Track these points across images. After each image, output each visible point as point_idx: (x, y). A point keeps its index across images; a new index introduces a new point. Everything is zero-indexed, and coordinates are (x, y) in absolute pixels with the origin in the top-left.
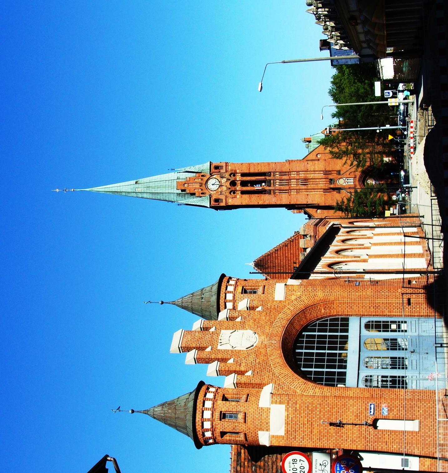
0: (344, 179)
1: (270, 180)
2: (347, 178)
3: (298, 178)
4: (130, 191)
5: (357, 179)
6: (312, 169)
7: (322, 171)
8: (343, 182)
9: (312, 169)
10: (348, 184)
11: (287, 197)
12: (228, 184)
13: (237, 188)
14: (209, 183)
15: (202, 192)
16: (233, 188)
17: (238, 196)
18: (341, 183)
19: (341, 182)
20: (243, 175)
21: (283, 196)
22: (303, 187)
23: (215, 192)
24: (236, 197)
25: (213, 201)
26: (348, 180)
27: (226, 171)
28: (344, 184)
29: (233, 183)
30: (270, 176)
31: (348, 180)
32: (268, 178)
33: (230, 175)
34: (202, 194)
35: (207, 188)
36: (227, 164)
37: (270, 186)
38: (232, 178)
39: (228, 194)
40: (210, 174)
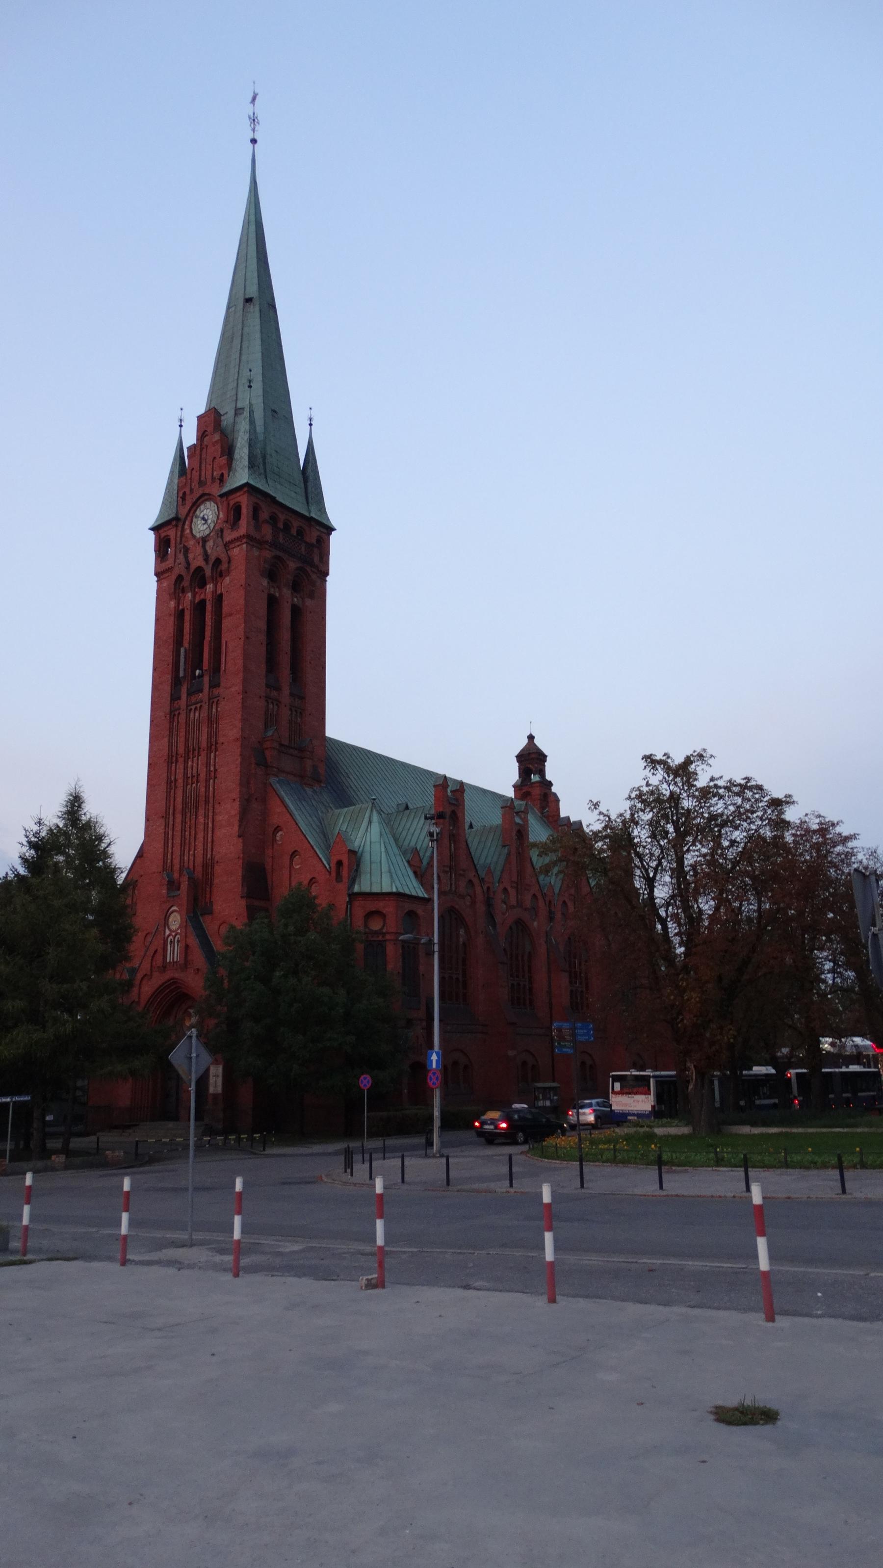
1: (201, 691)
3: (203, 776)
6: (221, 818)
9: (221, 818)
12: (199, 562)
15: (188, 492)
16: (186, 583)
23: (188, 531)
24: (171, 600)
27: (226, 545)
29: (199, 579)
32: (206, 679)
33: (218, 561)
34: (184, 493)
35: (196, 505)
36: (244, 540)
37: (189, 694)
38: (208, 572)
40: (221, 496)
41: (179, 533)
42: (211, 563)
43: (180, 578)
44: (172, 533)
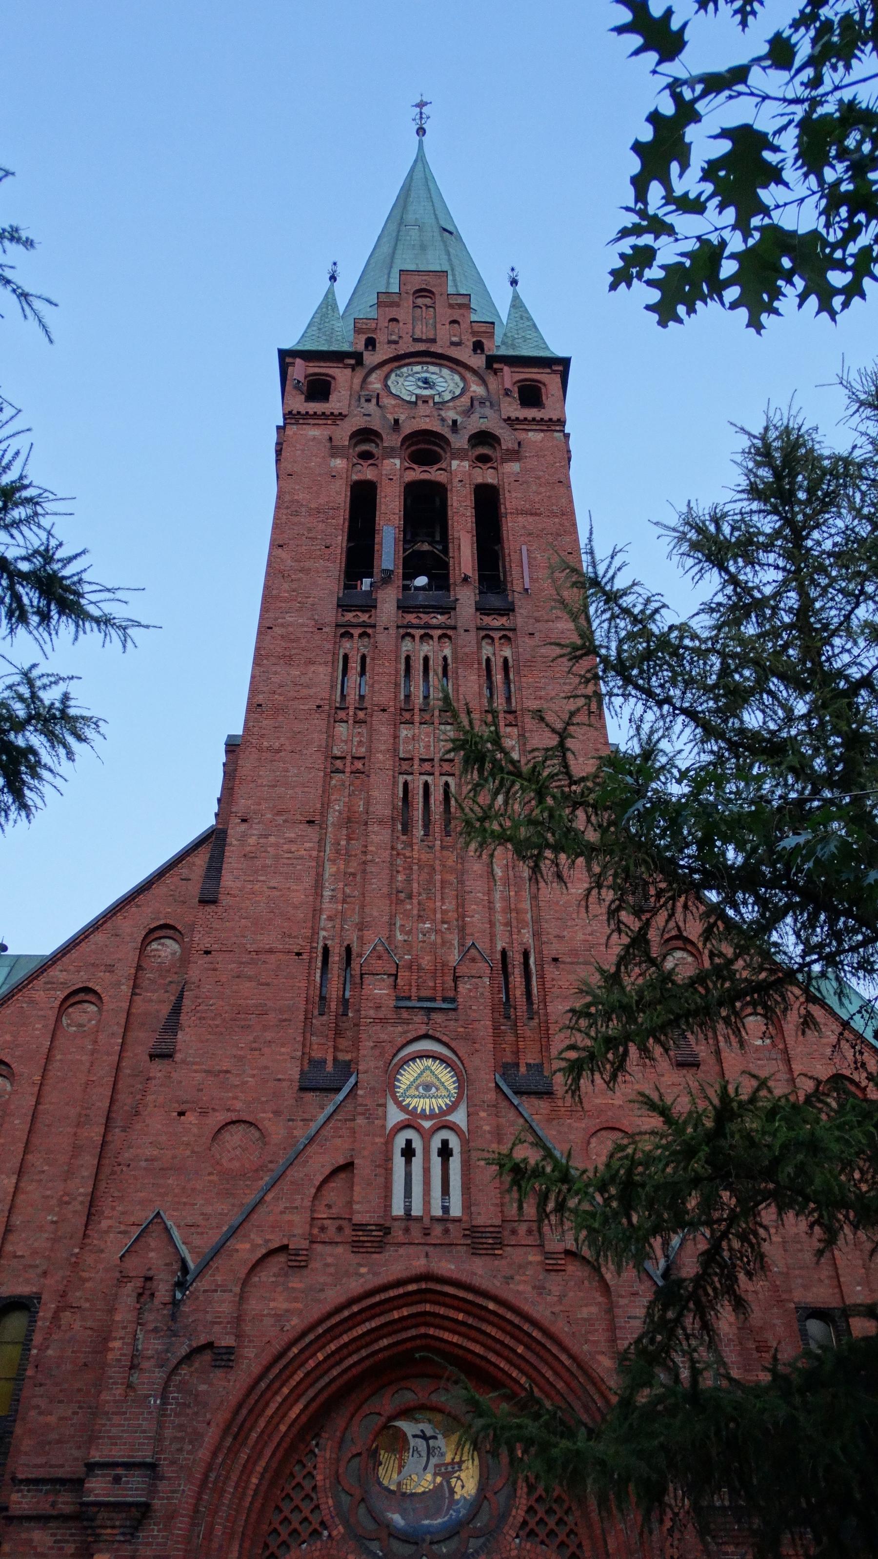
0: (459, 1118)
1: (448, 609)
2: (465, 1143)
4: (410, 217)
5: (446, 1266)
7: (537, 935)
8: (423, 1104)
10: (399, 1162)
11: (305, 692)
13: (397, 462)
14: (432, 368)
16: (392, 440)
17: (338, 463)
18: (408, 1077)
19: (426, 1085)
20: (487, 501)
21: (321, 669)
22: (382, 796)
23: (378, 386)
25: (317, 370)
26: (436, 1162)
27: (510, 421)
28: (395, 1116)
29: (425, 447)
30: (482, 609)
31: (445, 1152)
33: (483, 438)
35: (400, 360)
38: (460, 441)
39: (356, 422)
41: (357, 381)
42: (465, 435)
43: (365, 435)
44: (341, 376)
